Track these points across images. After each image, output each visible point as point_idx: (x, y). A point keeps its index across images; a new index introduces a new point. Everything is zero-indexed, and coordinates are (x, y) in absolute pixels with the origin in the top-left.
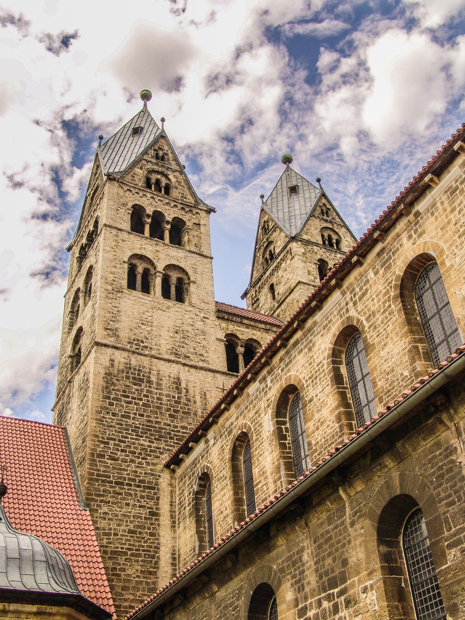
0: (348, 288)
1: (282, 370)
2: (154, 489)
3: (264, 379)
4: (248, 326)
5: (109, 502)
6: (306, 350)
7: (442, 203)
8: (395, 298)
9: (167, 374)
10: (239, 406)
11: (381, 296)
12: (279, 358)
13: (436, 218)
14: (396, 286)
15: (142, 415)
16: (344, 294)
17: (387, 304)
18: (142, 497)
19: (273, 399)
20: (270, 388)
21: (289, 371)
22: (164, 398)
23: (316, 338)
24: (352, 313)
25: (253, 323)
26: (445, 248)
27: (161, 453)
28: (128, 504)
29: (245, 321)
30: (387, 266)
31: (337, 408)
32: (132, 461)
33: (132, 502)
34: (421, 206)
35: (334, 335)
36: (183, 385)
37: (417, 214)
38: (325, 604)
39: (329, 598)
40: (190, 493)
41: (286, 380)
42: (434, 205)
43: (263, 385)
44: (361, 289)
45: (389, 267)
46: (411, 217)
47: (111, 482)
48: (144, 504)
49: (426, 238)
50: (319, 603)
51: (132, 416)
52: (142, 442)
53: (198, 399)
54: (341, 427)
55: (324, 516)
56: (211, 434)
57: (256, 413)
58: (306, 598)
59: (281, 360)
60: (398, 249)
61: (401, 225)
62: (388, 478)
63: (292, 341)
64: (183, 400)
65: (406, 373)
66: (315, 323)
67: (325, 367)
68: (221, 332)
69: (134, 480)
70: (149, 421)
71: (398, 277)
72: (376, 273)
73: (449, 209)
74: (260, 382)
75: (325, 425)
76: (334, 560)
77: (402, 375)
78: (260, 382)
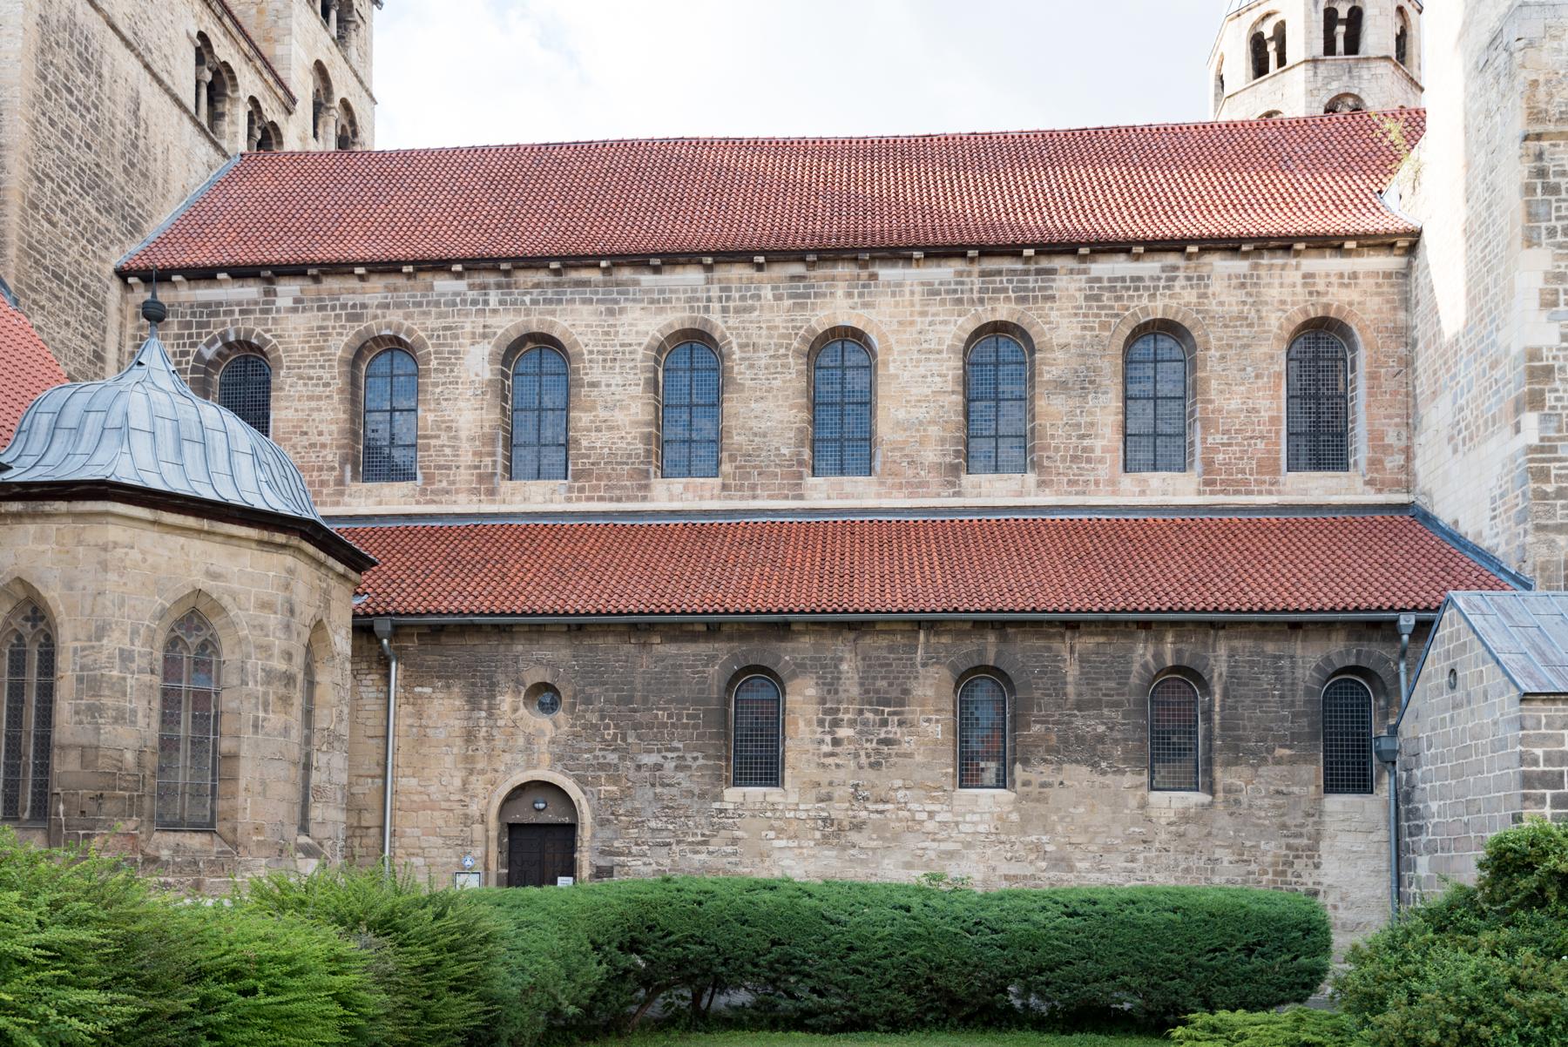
0: (720, 281)
1: (534, 302)
2: (100, 308)
3: (484, 287)
4: (227, 32)
5: (43, 308)
6: (603, 308)
7: (912, 293)
8: (798, 352)
9: (124, 74)
10: (396, 289)
11: (776, 333)
12: (536, 280)
13: (897, 305)
14: (804, 339)
15: (89, 146)
16: (709, 281)
17: (782, 351)
18: (86, 318)
19: (500, 332)
20: (495, 311)
21: (553, 313)
22: (119, 128)
23: (629, 305)
24: (716, 318)
25: (234, 31)
26: (896, 348)
27: (112, 242)
28: (67, 324)
29: (226, 20)
30: (801, 299)
31: (648, 424)
32: (74, 238)
33: (72, 320)
34: (886, 273)
35: (670, 325)
36: (142, 113)
37: (874, 276)
38: (869, 716)
39: (876, 712)
40: (184, 354)
41: (540, 322)
42: (900, 285)
43: (471, 295)
44: (743, 298)
45: (803, 306)
46: (864, 273)
47: (46, 269)
48: (88, 332)
49: (870, 314)
50: (861, 712)
51: (77, 141)
52: (88, 206)
53: (159, 156)
54: (648, 451)
55: (885, 643)
56: (288, 290)
57: (445, 328)
58: (839, 702)
59: (537, 285)
60: (824, 295)
61: (844, 270)
62: (990, 648)
63: (575, 275)
64: (141, 143)
65: (784, 451)
66: (636, 283)
67: (639, 357)
68: (194, 21)
69: (76, 279)
70: (98, 165)
71: (811, 330)
72: (778, 298)
73: (918, 308)
74: (471, 287)
75: (616, 434)
76: (890, 685)
77: (778, 449)
78: (471, 287)
